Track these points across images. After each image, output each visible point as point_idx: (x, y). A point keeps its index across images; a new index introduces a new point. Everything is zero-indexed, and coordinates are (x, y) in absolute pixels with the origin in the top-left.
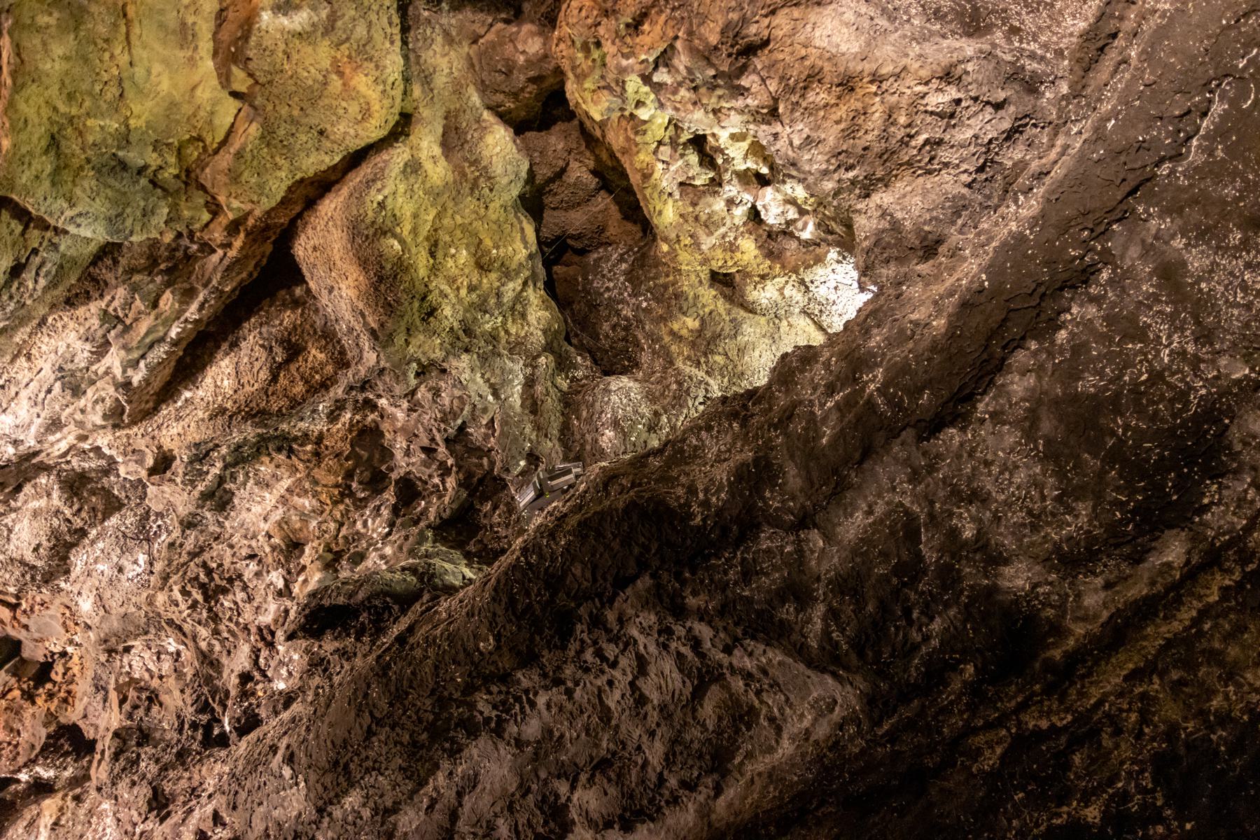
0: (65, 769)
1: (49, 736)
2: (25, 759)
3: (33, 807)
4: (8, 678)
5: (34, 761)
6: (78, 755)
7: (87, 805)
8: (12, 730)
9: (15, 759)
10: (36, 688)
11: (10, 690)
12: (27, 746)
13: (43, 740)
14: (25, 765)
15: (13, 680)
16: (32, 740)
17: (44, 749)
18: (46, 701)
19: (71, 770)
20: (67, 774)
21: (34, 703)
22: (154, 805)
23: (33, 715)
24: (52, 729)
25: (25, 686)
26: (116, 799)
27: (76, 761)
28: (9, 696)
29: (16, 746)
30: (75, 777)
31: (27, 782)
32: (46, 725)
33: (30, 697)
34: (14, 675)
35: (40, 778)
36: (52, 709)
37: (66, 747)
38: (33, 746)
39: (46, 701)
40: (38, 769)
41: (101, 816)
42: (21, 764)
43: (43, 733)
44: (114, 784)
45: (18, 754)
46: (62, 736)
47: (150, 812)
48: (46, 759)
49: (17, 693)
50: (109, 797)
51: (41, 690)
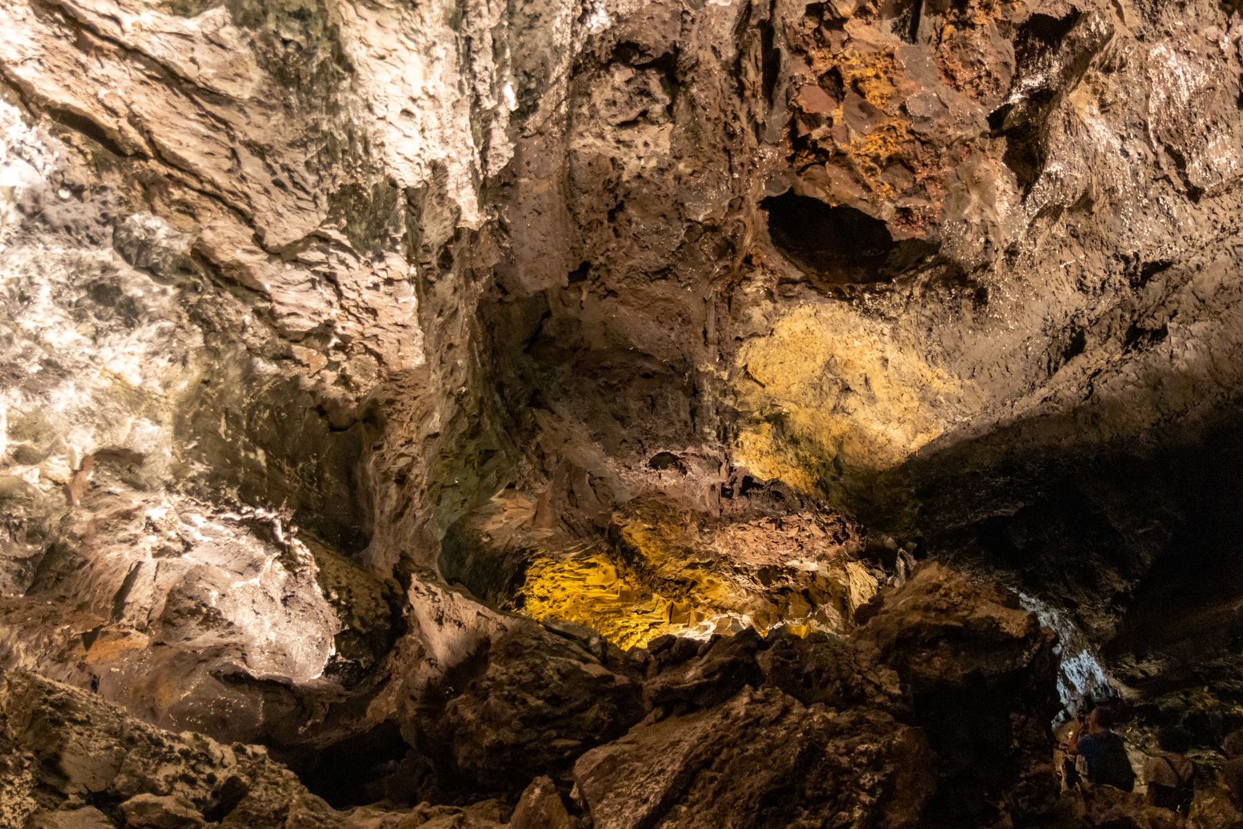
0: (1050, 66)
1: (1016, 44)
2: (1009, 79)
3: (1054, 112)
4: (933, 20)
5: (1018, 76)
6: (1053, 46)
7: (1132, 63)
8: (972, 64)
9: (998, 86)
10: (963, 12)
11: (942, 30)
12: (999, 68)
13: (1012, 51)
14: (1013, 84)
15: (939, 19)
16: (1002, 58)
17: (1019, 57)
18: (987, 14)
19: (1056, 64)
20: (1056, 68)
21: (973, 26)
22: (1229, 7)
23: (984, 35)
24: (1014, 34)
25: (952, 18)
26: (1168, 34)
27: (1054, 53)
28: (945, 37)
29: (989, 74)
30: (1066, 67)
31: (1022, 101)
32: (1005, 35)
33: (965, 24)
34: (936, 13)
35: (1032, 90)
36: (1000, 17)
37: (1037, 44)
38: (1006, 64)
39: (987, 14)
40: (1025, 82)
41: (1157, 64)
42: (1008, 85)
43: (1008, 44)
44: (1154, 23)
45: (997, 80)
46: (1026, 38)
47: (1230, 16)
48: (1027, 67)
49: (950, 29)
50: (1159, 37)
51: (969, 11)
